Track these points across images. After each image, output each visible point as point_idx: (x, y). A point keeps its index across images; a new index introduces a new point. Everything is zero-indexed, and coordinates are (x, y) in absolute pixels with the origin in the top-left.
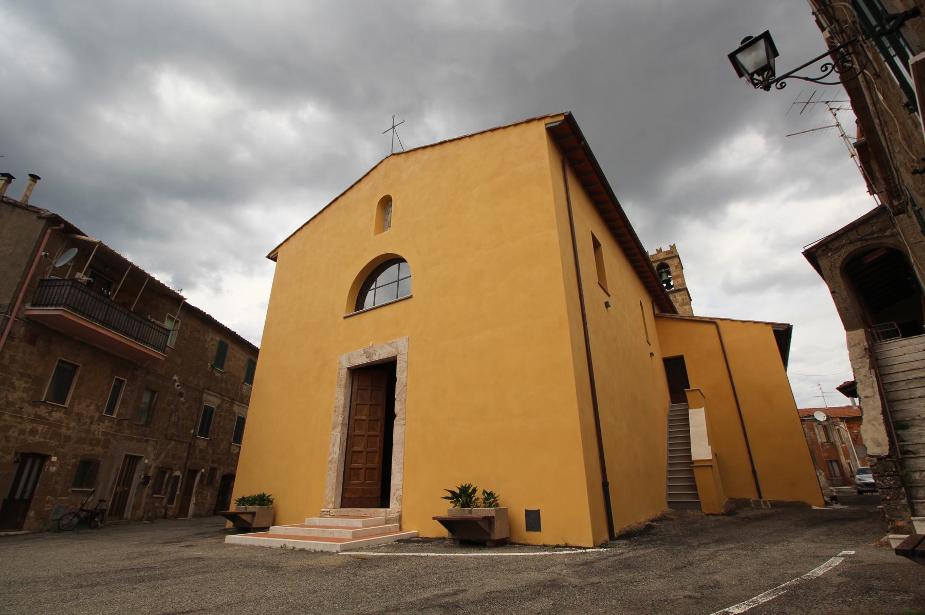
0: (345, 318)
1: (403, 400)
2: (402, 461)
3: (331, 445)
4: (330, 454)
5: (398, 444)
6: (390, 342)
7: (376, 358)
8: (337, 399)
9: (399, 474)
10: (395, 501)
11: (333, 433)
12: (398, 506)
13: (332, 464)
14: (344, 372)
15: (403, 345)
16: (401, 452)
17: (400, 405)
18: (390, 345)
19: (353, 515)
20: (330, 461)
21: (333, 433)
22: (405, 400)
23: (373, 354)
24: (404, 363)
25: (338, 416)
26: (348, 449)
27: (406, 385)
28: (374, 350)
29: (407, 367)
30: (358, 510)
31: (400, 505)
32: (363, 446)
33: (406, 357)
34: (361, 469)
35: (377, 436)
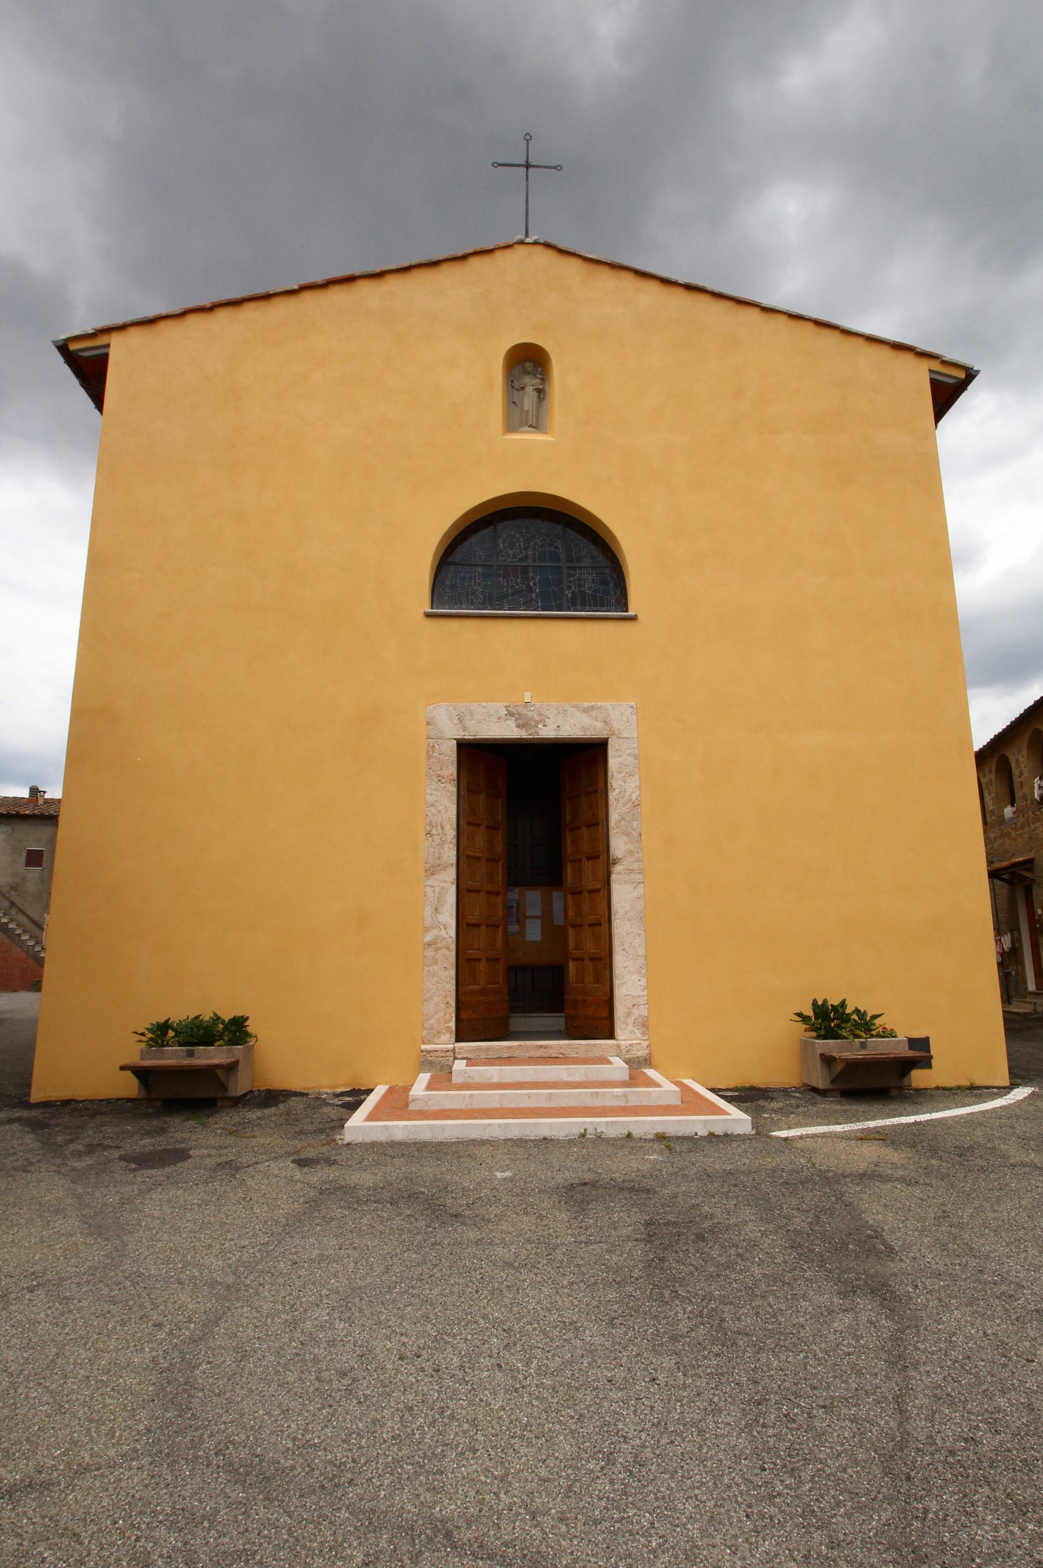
0: (428, 615)
1: (635, 834)
2: (642, 952)
3: (428, 911)
4: (427, 930)
5: (629, 920)
6: (586, 704)
7: (548, 732)
8: (432, 805)
9: (636, 977)
10: (630, 1027)
11: (429, 882)
12: (639, 1035)
13: (437, 950)
14: (450, 750)
15: (625, 719)
16: (639, 935)
17: (626, 843)
18: (586, 711)
19: (528, 1055)
20: (430, 944)
21: (429, 882)
22: (640, 834)
23: (537, 722)
24: (631, 759)
25: (441, 845)
26: (460, 920)
27: (639, 805)
28: (541, 714)
29: (639, 767)
30: (541, 1047)
31: (643, 1034)
32: (478, 913)
33: (635, 746)
34: (479, 960)
35: (497, 894)
